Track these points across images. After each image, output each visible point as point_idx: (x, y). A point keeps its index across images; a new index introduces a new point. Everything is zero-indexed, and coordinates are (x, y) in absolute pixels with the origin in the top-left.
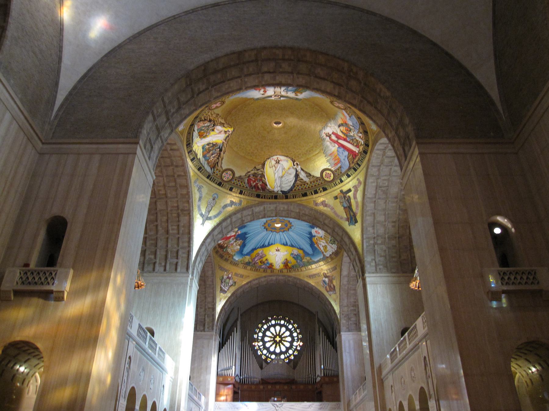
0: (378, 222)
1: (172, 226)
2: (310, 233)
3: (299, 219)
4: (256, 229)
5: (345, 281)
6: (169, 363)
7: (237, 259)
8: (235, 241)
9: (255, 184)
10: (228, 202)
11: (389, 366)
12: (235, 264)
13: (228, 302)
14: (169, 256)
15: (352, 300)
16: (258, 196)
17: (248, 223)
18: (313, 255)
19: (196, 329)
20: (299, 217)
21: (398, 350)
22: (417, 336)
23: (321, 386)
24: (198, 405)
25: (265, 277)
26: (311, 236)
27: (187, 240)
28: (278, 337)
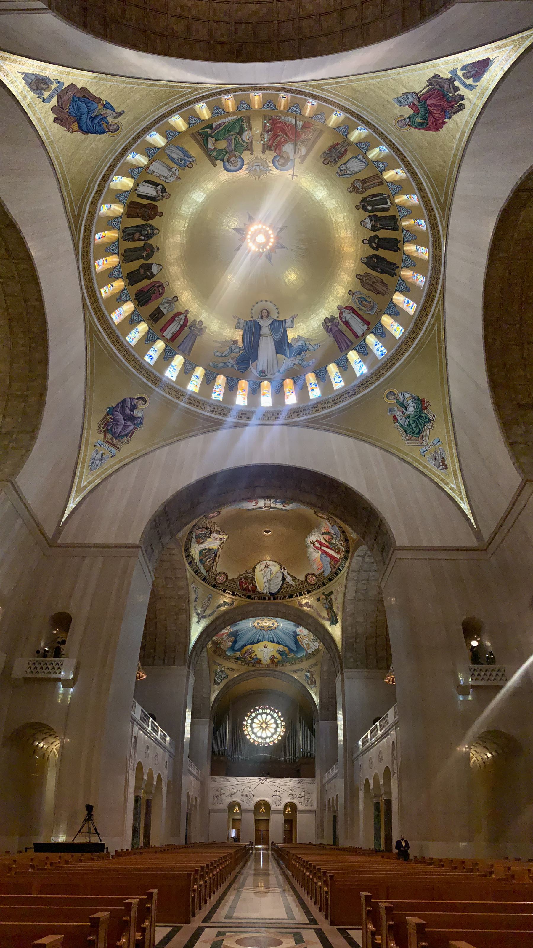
7: (229, 655)
8: (228, 638)
10: (222, 602)
12: (227, 658)
16: (249, 597)
18: (297, 652)
25: (254, 671)
26: (296, 635)
28: (264, 724)
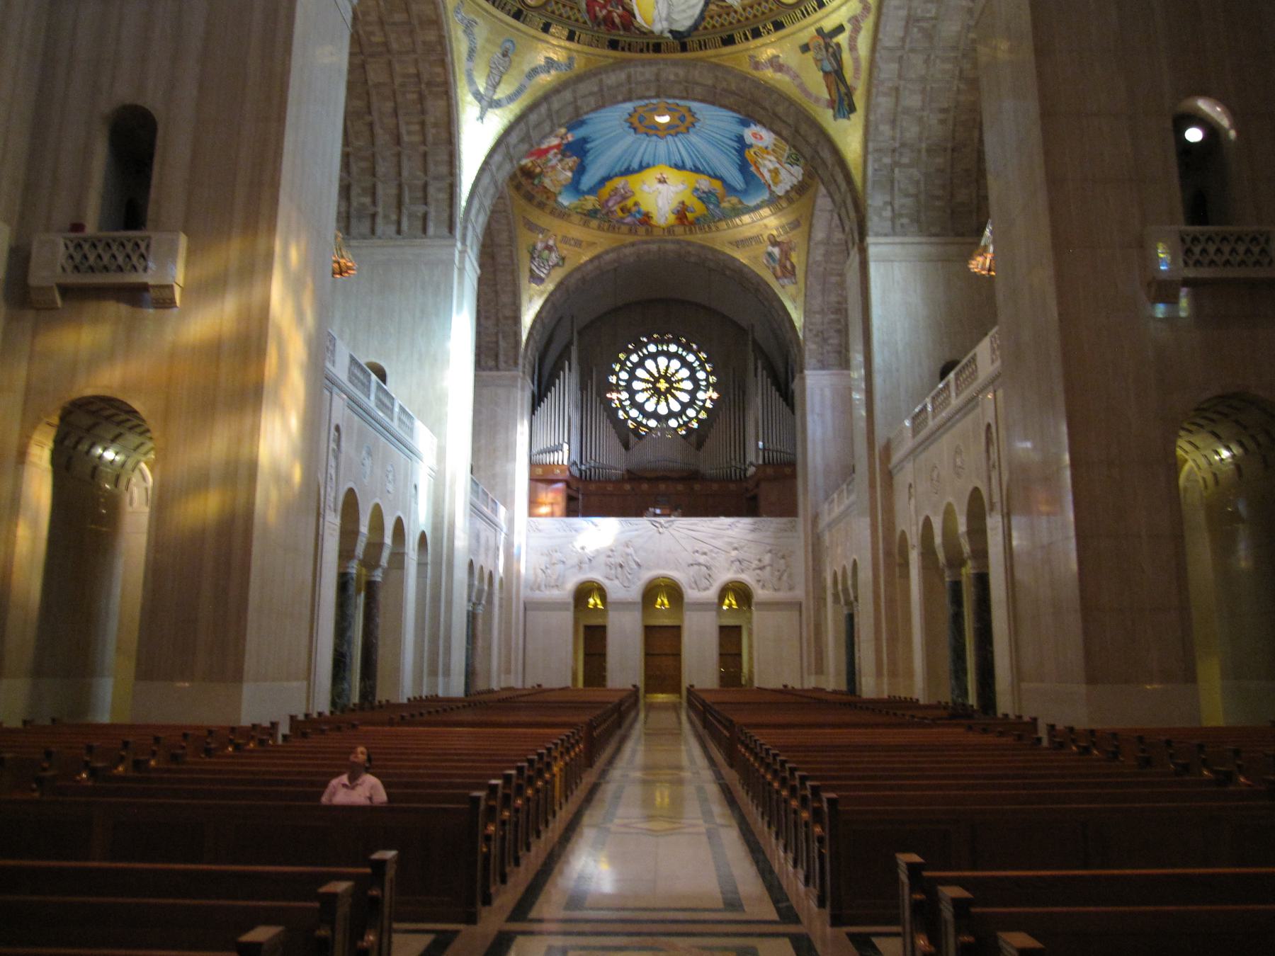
0: (907, 111)
1: (408, 123)
2: (740, 139)
3: (713, 103)
4: (610, 128)
5: (818, 254)
6: (423, 438)
7: (566, 203)
8: (561, 161)
9: (604, 12)
11: (909, 443)
12: (563, 214)
13: (549, 304)
14: (406, 199)
15: (833, 298)
16: (613, 45)
17: (591, 116)
18: (745, 192)
19: (479, 365)
20: (713, 99)
21: (929, 408)
22: (976, 379)
23: (757, 485)
24: (493, 524)
25: (633, 244)
27: (446, 158)
